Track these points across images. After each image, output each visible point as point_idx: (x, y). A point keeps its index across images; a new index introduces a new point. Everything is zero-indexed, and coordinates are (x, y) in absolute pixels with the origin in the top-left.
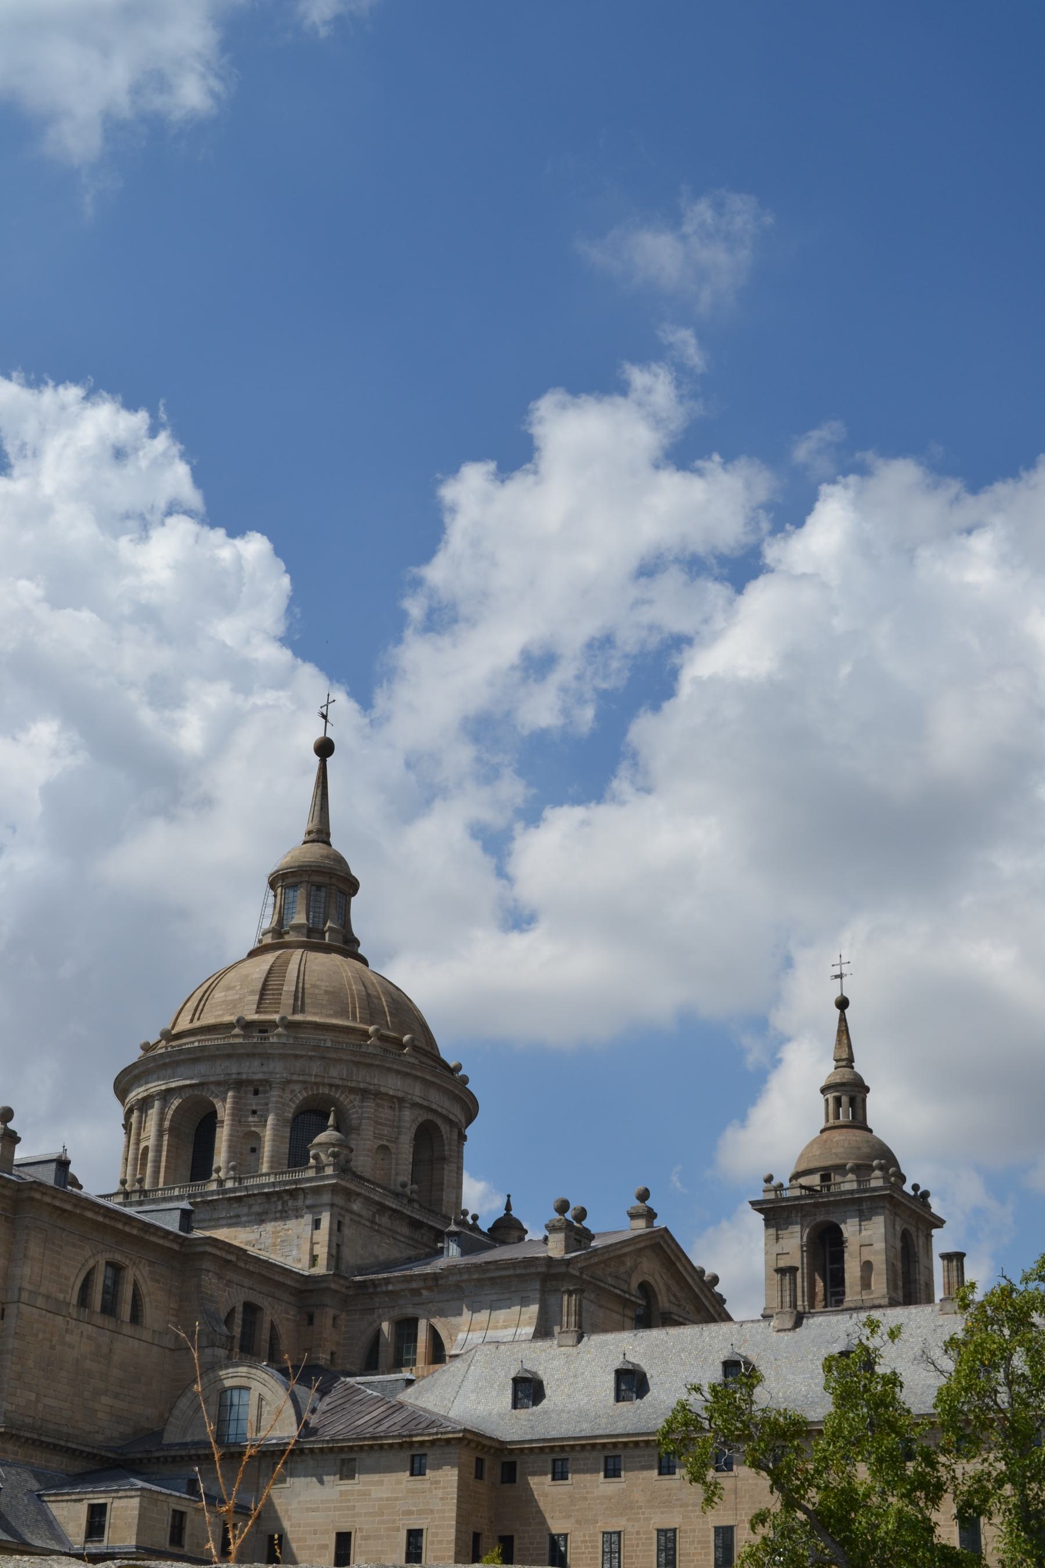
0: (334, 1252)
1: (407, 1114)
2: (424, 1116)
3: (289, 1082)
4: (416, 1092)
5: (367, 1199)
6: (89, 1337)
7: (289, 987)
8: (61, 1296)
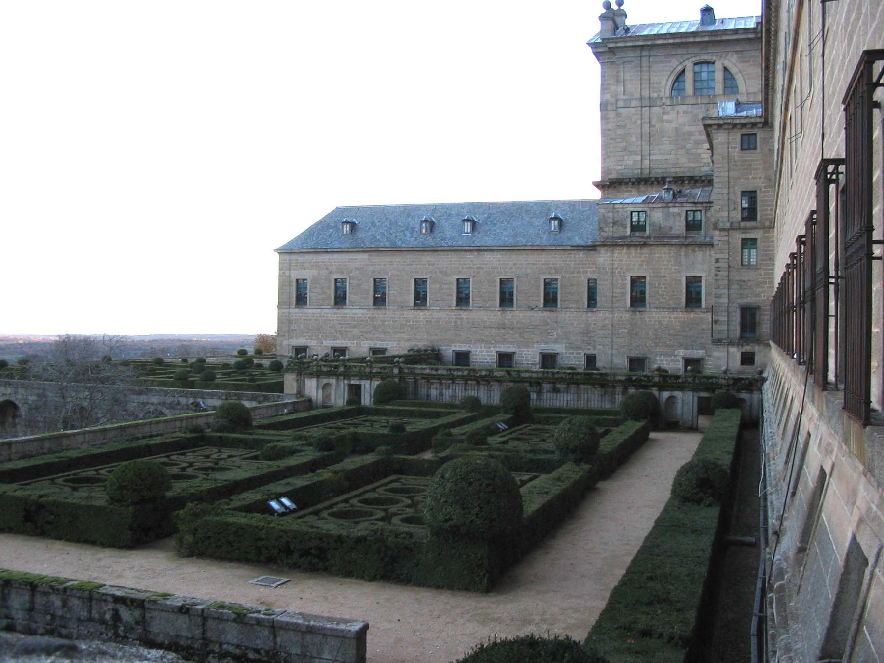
6: (685, 112)
8: (655, 95)
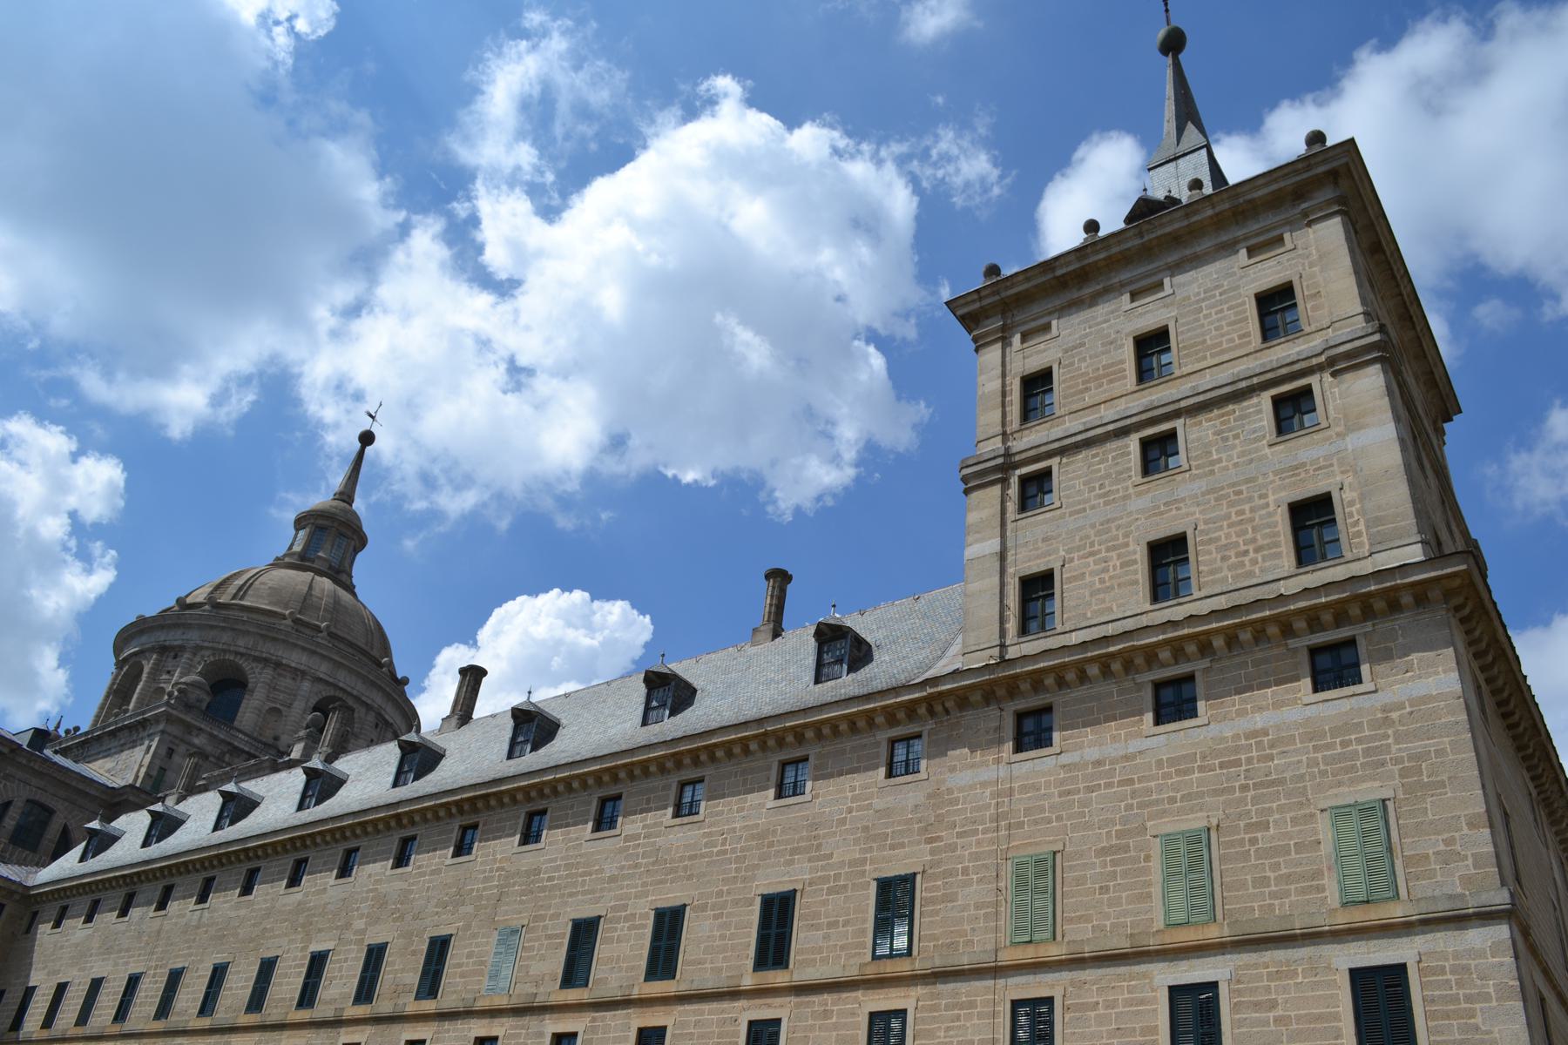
0: (154, 773)
1: (306, 685)
2: (331, 692)
3: (202, 648)
4: (323, 669)
5: (211, 735)
7: (240, 582)
